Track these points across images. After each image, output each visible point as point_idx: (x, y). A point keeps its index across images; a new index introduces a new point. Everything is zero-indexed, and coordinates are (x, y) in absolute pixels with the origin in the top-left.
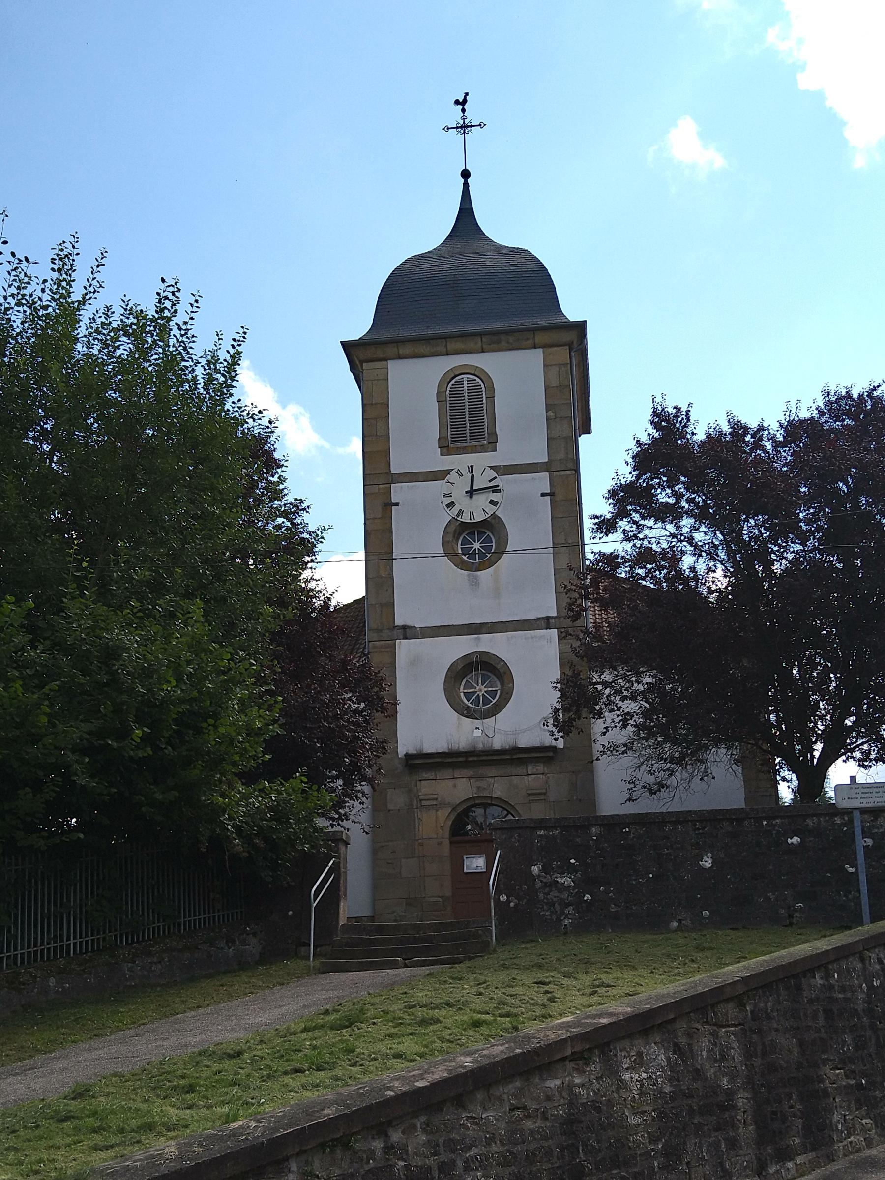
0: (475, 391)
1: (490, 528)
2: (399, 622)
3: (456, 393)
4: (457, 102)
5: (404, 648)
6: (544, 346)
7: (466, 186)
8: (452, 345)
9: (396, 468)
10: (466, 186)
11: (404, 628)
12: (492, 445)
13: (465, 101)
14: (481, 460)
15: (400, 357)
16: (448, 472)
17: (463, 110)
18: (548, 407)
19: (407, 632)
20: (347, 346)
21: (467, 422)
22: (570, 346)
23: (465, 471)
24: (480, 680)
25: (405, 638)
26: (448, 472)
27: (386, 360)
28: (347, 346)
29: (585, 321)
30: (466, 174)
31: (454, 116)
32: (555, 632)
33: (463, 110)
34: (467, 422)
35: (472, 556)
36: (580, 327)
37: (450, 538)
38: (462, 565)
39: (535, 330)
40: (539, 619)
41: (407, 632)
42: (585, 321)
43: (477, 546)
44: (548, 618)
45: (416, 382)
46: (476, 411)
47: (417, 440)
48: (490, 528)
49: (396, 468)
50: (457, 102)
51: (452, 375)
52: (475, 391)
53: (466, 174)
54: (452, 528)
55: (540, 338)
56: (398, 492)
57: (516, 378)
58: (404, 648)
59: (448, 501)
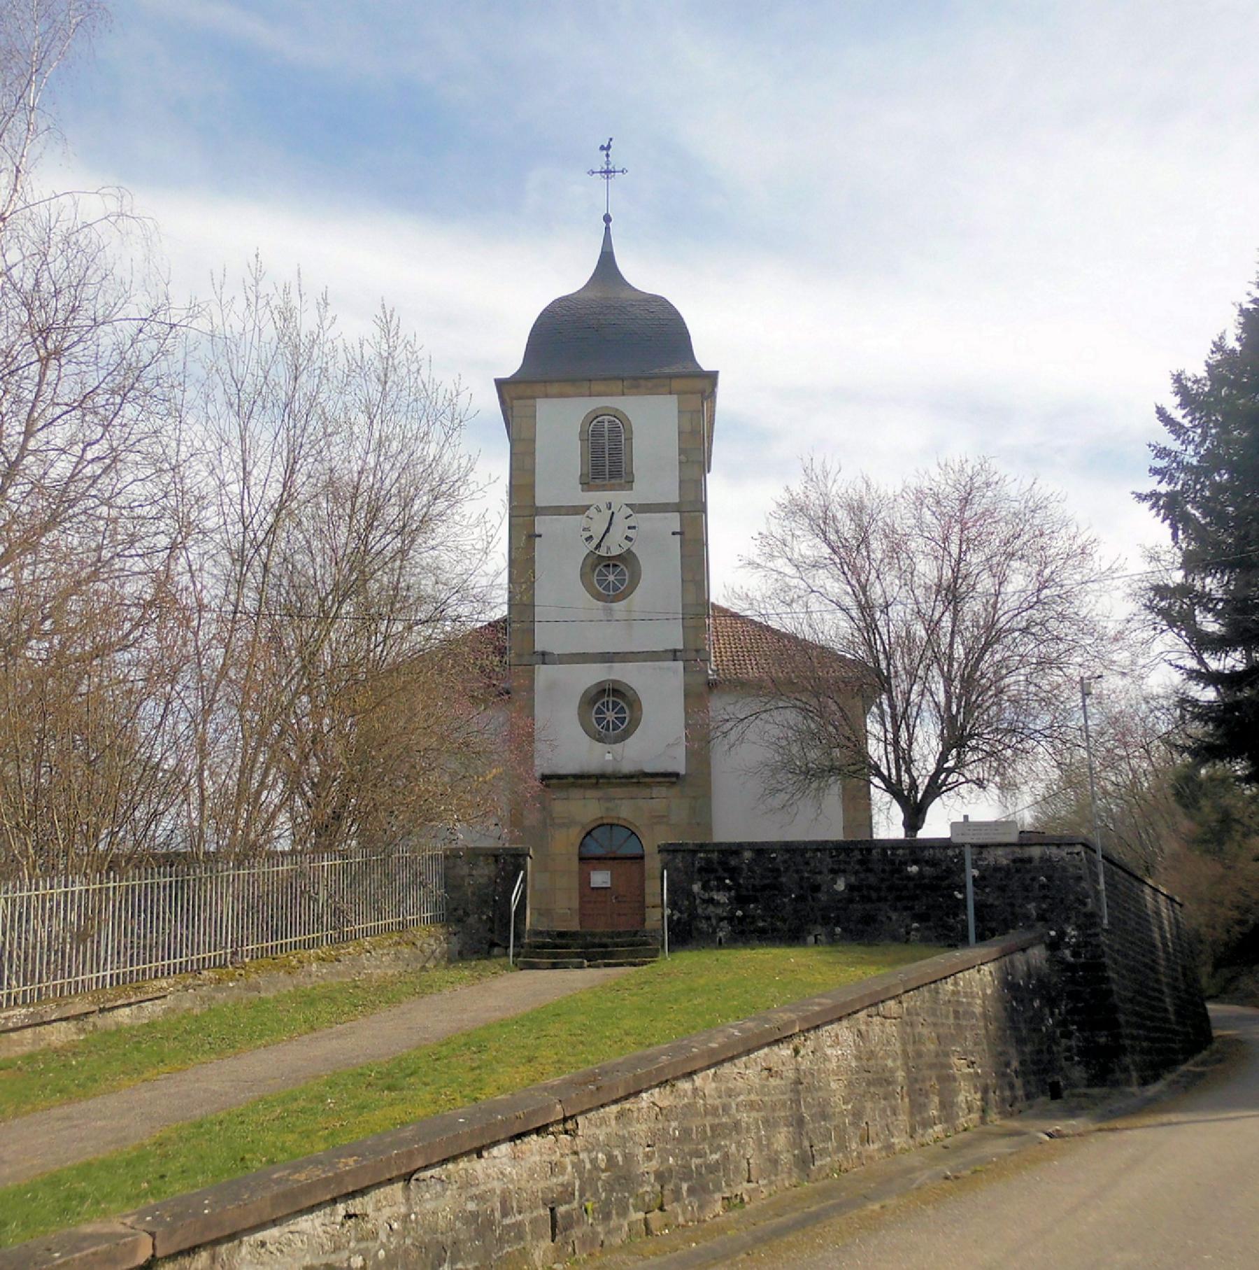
0: (614, 431)
1: (626, 561)
2: (538, 648)
3: (597, 434)
4: (602, 148)
5: (543, 673)
6: (679, 393)
7: (607, 229)
8: (597, 387)
9: (541, 501)
10: (607, 229)
11: (543, 654)
12: (629, 484)
13: (609, 147)
14: (619, 498)
15: (547, 396)
16: (588, 507)
17: (607, 156)
18: (682, 451)
19: (545, 658)
20: (500, 384)
21: (606, 461)
22: (702, 393)
23: (603, 507)
24: (611, 708)
25: (544, 663)
26: (588, 507)
27: (534, 398)
28: (500, 384)
29: (716, 373)
30: (607, 219)
31: (599, 162)
32: (681, 664)
33: (607, 156)
34: (606, 461)
35: (607, 588)
36: (712, 377)
37: (588, 569)
38: (598, 597)
39: (671, 377)
40: (666, 651)
41: (545, 658)
42: (716, 373)
43: (611, 578)
44: (675, 651)
45: (562, 421)
46: (616, 451)
47: (561, 472)
48: (626, 561)
49: (541, 501)
50: (602, 148)
51: (595, 416)
52: (614, 431)
53: (607, 219)
54: (590, 561)
55: (676, 384)
56: (542, 524)
57: (651, 420)
58: (543, 673)
59: (587, 534)
